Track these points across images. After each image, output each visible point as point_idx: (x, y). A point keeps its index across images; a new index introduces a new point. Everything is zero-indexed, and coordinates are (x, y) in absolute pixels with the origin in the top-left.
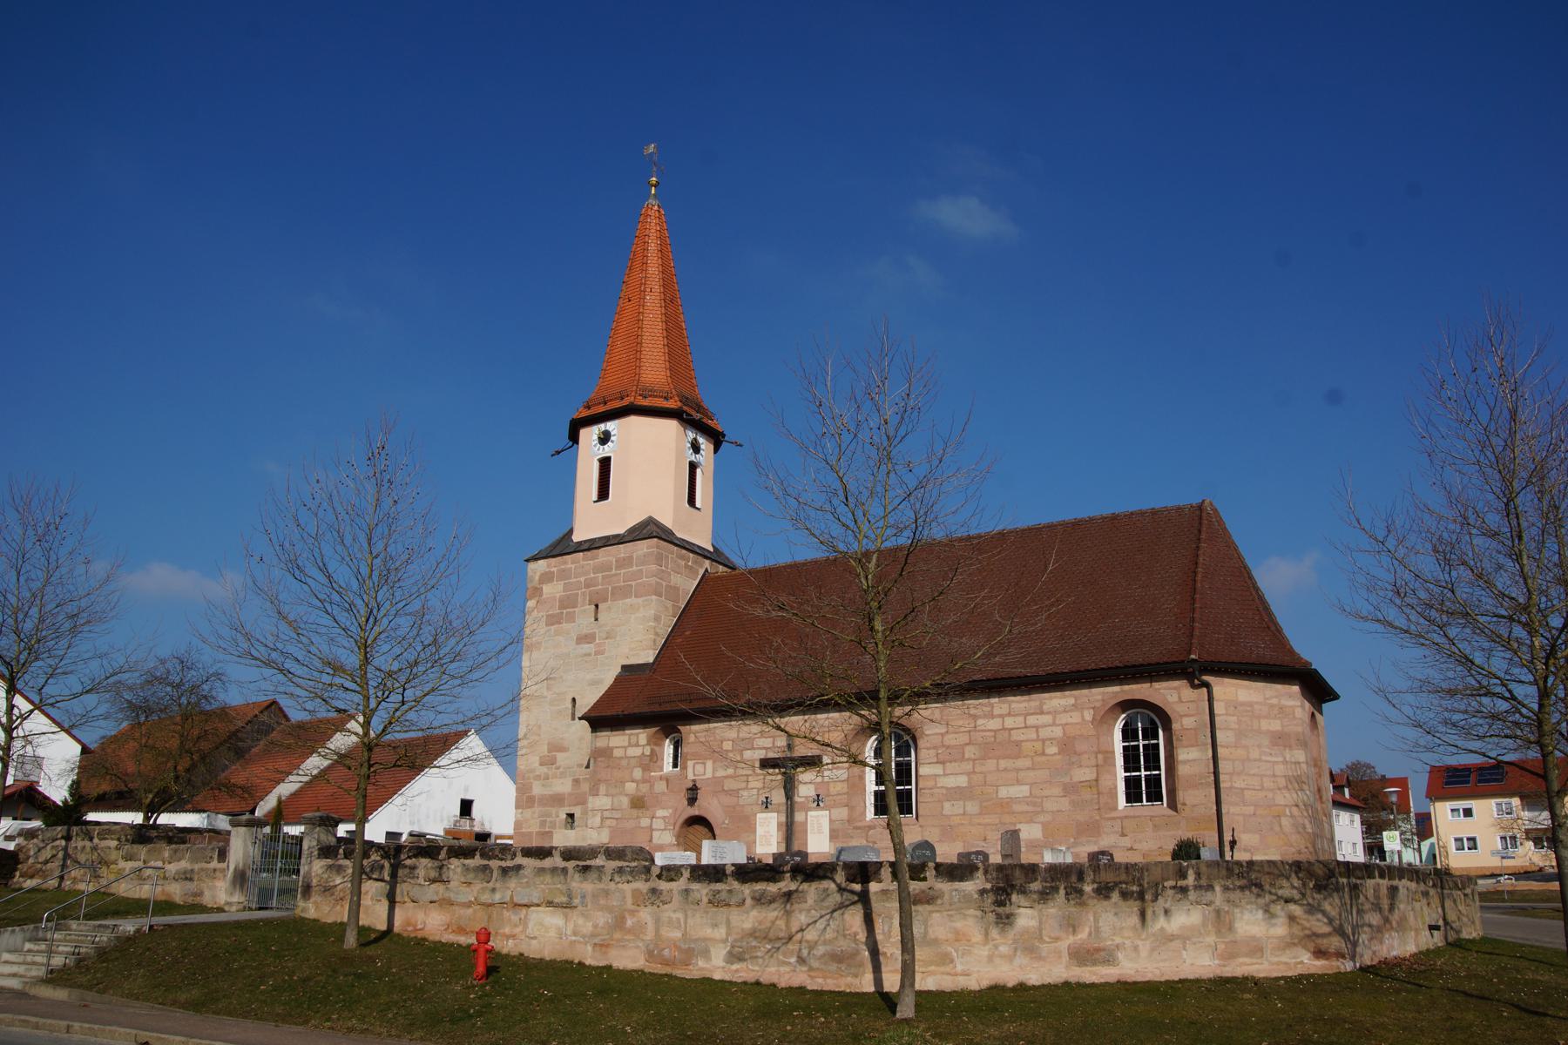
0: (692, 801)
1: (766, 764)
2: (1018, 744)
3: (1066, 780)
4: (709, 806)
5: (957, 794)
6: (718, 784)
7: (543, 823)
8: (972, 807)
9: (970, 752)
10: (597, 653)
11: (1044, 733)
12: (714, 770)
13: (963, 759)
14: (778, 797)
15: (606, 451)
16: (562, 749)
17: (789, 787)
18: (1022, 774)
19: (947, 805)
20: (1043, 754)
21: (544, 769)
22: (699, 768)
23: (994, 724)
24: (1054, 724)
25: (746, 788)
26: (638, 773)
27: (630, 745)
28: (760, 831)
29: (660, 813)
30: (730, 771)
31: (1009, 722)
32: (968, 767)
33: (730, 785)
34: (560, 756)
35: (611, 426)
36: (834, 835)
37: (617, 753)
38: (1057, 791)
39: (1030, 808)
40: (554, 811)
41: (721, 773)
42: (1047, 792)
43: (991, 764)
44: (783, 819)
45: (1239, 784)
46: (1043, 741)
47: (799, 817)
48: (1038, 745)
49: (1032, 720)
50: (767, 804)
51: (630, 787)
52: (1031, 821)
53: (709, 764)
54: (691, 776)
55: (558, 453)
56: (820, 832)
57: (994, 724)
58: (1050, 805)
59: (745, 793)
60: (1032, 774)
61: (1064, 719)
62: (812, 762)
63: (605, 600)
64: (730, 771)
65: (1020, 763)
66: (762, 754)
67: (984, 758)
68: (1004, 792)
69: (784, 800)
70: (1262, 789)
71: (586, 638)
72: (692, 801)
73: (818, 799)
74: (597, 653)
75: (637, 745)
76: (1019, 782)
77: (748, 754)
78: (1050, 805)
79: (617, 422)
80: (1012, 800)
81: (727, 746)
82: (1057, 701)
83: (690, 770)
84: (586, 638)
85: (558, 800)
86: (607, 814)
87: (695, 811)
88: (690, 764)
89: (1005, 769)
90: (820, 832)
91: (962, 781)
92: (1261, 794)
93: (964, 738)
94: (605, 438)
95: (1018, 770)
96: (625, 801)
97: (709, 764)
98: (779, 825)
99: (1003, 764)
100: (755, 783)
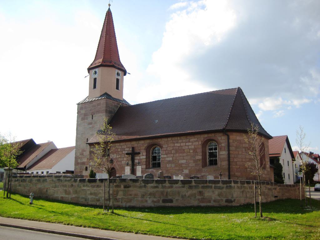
1: (127, 154)
2: (184, 150)
3: (194, 159)
4: (116, 165)
5: (169, 162)
7: (81, 169)
8: (173, 165)
9: (173, 152)
10: (93, 127)
11: (190, 147)
12: (116, 156)
13: (171, 153)
14: (130, 163)
15: (96, 76)
17: (133, 160)
18: (184, 157)
19: (167, 165)
20: (189, 152)
22: (113, 155)
23: (178, 145)
24: (192, 145)
31: (182, 144)
32: (172, 155)
33: (120, 159)
34: (84, 153)
35: (97, 70)
38: (192, 161)
39: (186, 166)
40: (83, 166)
41: (117, 157)
42: (190, 162)
43: (178, 154)
45: (235, 160)
46: (190, 149)
48: (188, 150)
49: (187, 144)
50: (128, 165)
52: (186, 169)
53: (115, 154)
54: (111, 158)
55: (86, 77)
57: (178, 145)
58: (190, 165)
59: (123, 162)
60: (187, 157)
61: (194, 144)
63: (94, 114)
64: (120, 156)
65: (185, 154)
66: (126, 152)
67: (176, 153)
68: (180, 162)
70: (242, 161)
71: (90, 124)
73: (139, 163)
74: (93, 127)
76: (184, 159)
77: (124, 152)
78: (190, 165)
80: (182, 164)
81: (119, 150)
82: (193, 139)
83: (111, 156)
84: (90, 124)
85: (83, 163)
86: (93, 167)
88: (111, 154)
89: (181, 156)
91: (171, 159)
92: (242, 163)
93: (172, 148)
94: (96, 73)
95: (183, 156)
97: (115, 154)
99: (180, 155)
100: (125, 159)
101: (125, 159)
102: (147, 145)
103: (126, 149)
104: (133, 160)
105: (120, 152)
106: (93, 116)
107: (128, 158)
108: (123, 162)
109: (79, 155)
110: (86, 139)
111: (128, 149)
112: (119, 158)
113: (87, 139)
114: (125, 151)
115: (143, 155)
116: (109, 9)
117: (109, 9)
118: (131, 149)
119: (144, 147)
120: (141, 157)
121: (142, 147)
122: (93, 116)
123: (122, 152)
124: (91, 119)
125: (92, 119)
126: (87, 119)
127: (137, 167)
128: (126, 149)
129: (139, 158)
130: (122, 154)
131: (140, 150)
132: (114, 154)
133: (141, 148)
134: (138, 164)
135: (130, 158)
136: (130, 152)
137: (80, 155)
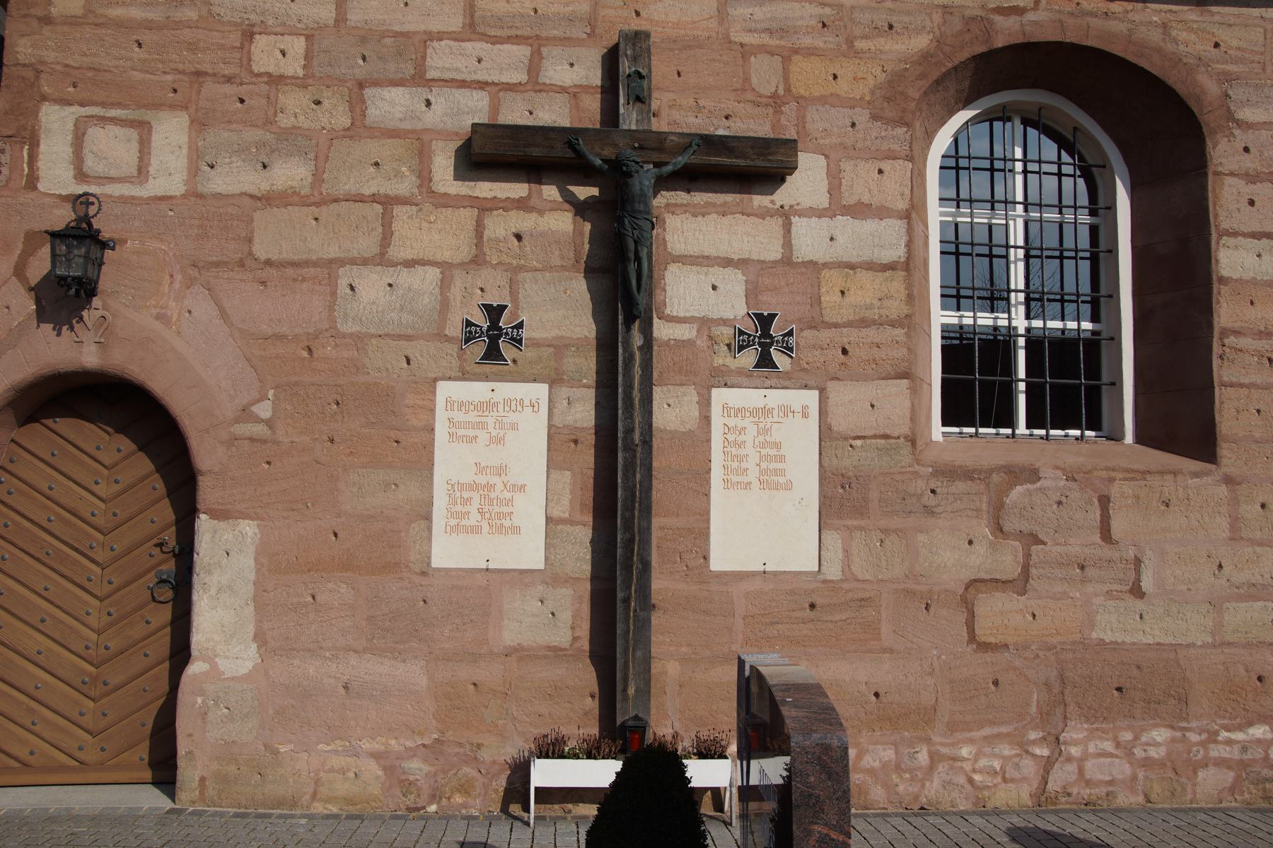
0: (66, 297)
1: (496, 154)
6: (218, 238)
12: (199, 161)
14: (561, 311)
17: (621, 279)
22: (112, 147)
25: (381, 259)
28: (452, 462)
30: (291, 173)
36: (841, 499)
41: (235, 178)
44: (583, 413)
47: (671, 410)
50: (493, 341)
53: (171, 132)
54: (56, 175)
56: (774, 480)
59: (372, 289)
62: (745, 168)
64: (291, 173)
69: (585, 327)
72: (66, 297)
77: (391, 104)
87: (78, 350)
88: (56, 122)
90: (774, 480)
97: (171, 132)
98: (559, 441)
101: (443, 236)
102: (921, 42)
104: (621, 279)
105: (294, 103)
107: (499, 227)
111: (507, 63)
112: (267, 200)
114: (419, 79)
118: (578, 70)
119: (874, 75)
120: (811, 240)
121: (811, 52)
123: (357, 105)
127: (720, 396)
128: (442, 60)
129: (773, 252)
130: (359, 128)
131: (776, 102)
132: (143, 128)
133: (800, 66)
134: (749, 358)
135: (551, 219)
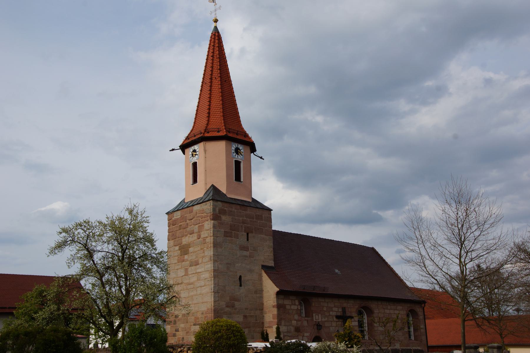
1: (338, 317)
15: (239, 158)
16: (238, 300)
21: (227, 309)
22: (317, 317)
26: (296, 317)
27: (292, 304)
29: (306, 334)
34: (237, 303)
35: (241, 147)
37: (288, 307)
41: (323, 320)
51: (294, 322)
53: (320, 315)
54: (315, 320)
63: (252, 232)
64: (326, 319)
66: (334, 314)
75: (295, 305)
77: (331, 313)
79: (243, 146)
83: (314, 317)
86: (285, 334)
88: (314, 314)
96: (293, 329)
97: (320, 315)
100: (334, 324)
103: (334, 309)
106: (248, 234)
107: (338, 323)
108: (331, 328)
109: (224, 306)
110: (238, 277)
111: (336, 309)
112: (326, 321)
113: (240, 277)
115: (355, 321)
116: (216, 27)
117: (216, 27)
118: (340, 310)
122: (248, 234)
124: (246, 239)
125: (248, 240)
126: (237, 237)
136: (339, 314)
137: (227, 307)
